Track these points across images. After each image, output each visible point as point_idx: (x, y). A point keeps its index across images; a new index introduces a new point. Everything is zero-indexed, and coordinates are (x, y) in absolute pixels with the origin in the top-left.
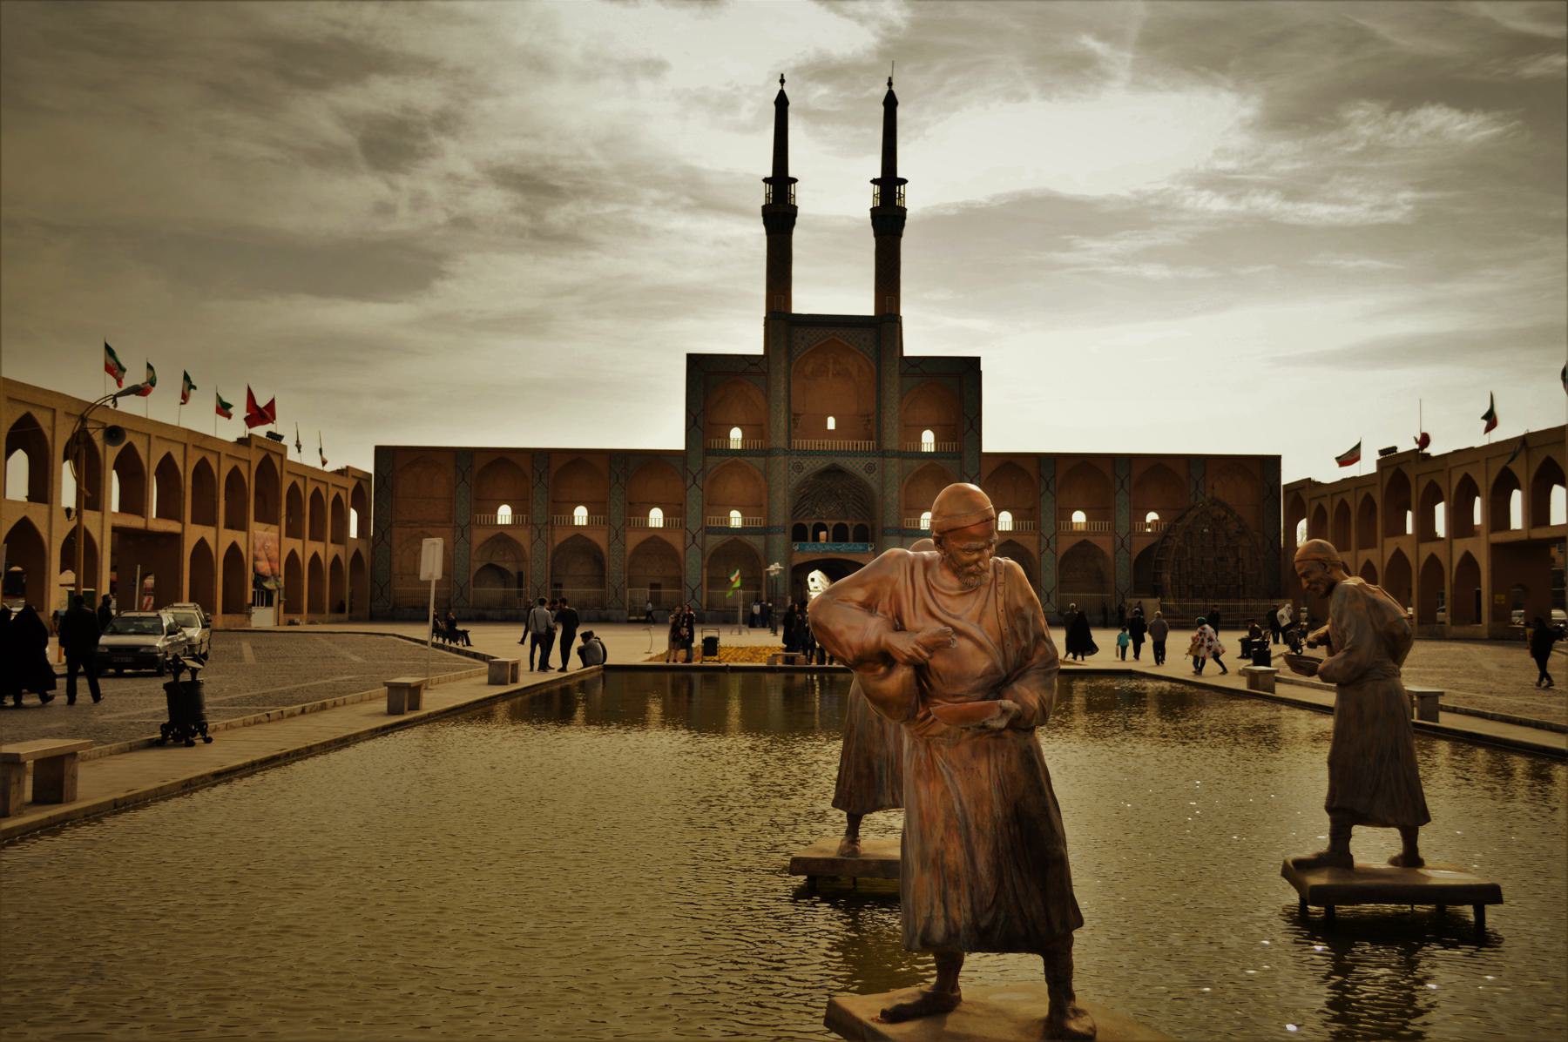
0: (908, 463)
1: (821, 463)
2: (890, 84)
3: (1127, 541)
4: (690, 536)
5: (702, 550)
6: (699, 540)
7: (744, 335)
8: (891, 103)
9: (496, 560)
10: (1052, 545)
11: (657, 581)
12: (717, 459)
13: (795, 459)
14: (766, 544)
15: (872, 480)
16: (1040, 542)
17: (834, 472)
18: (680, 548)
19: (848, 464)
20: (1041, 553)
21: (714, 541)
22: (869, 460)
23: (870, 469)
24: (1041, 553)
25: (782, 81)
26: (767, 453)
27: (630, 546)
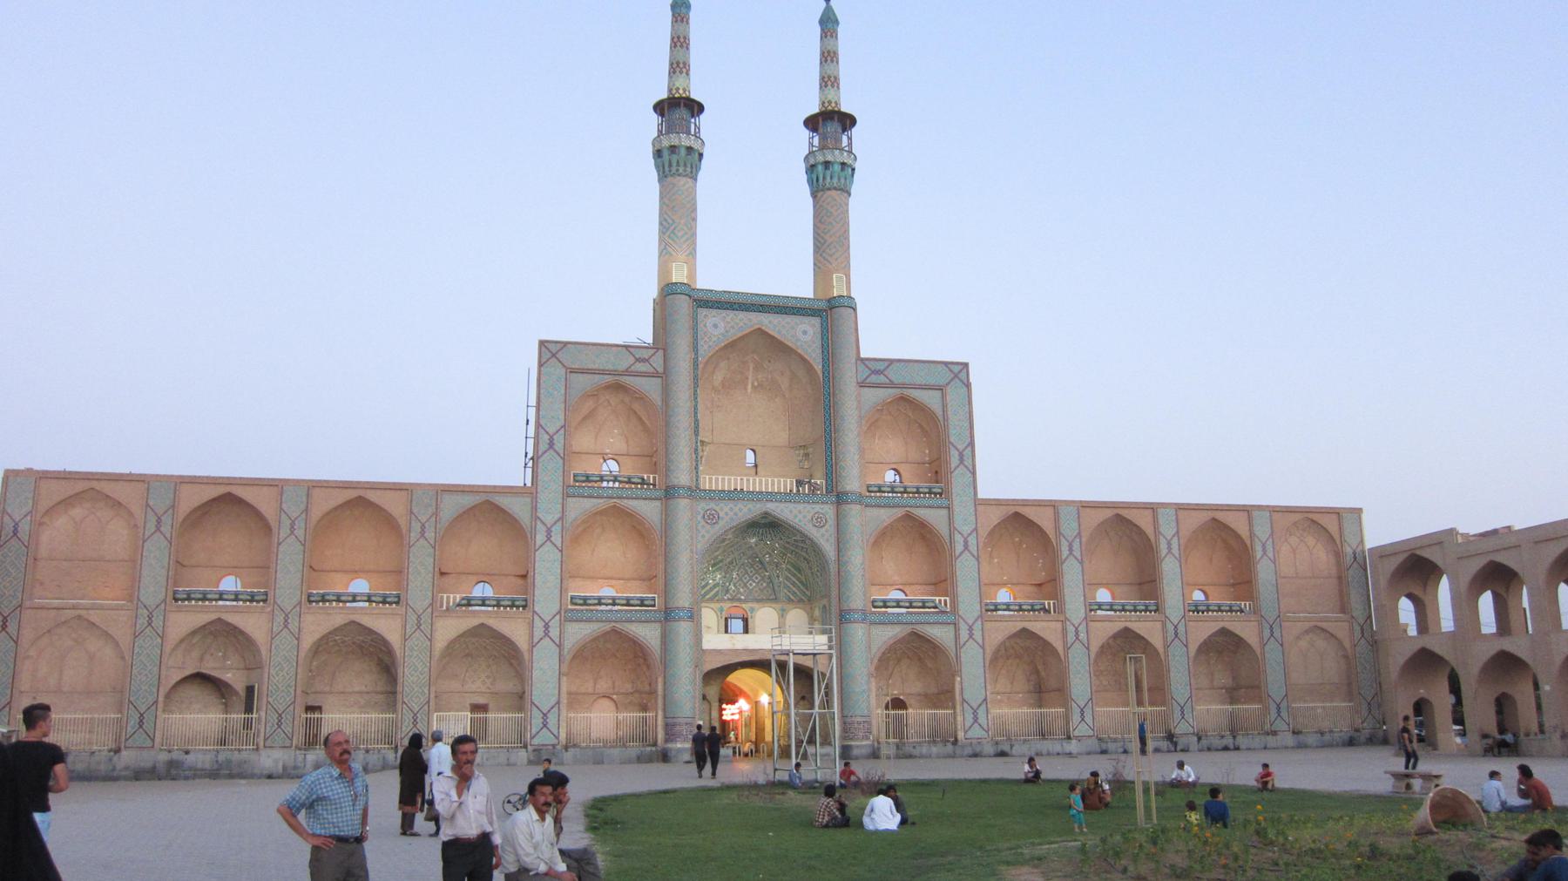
0: (875, 511)
3: (1181, 629)
4: (539, 624)
5: (560, 646)
6: (554, 633)
8: (828, 23)
9: (209, 668)
10: (1082, 636)
11: (481, 700)
13: (702, 506)
14: (665, 639)
18: (521, 641)
19: (784, 511)
20: (1067, 648)
21: (578, 633)
22: (818, 507)
23: (819, 522)
26: (669, 493)
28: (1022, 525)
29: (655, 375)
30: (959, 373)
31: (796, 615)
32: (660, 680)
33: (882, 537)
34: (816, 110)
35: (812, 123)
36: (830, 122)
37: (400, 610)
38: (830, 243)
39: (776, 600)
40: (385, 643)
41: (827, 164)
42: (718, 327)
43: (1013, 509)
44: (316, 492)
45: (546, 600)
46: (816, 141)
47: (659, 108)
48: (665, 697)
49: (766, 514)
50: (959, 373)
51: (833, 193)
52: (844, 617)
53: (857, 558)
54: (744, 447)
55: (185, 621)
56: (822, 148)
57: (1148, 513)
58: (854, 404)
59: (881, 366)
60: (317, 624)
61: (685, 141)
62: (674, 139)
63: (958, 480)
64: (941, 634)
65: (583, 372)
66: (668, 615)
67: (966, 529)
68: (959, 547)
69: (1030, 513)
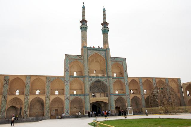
0: (113, 79)
1: (95, 79)
2: (104, 7)
4: (66, 97)
6: (68, 98)
7: (77, 51)
8: (104, 11)
9: (14, 105)
10: (143, 97)
12: (72, 78)
15: (107, 83)
16: (141, 96)
17: (98, 81)
18: (63, 99)
21: (72, 98)
23: (106, 81)
24: (142, 99)
25: (84, 4)
27: (51, 100)
28: (134, 81)
29: (82, 59)
30: (124, 59)
31: (102, 95)
32: (84, 105)
33: (115, 83)
34: (103, 22)
35: (102, 24)
36: (105, 24)
37: (45, 95)
38: (106, 41)
39: (99, 92)
40: (42, 100)
41: (105, 30)
42: (91, 53)
43: (133, 79)
44: (32, 77)
45: (67, 92)
46: (103, 27)
47: (81, 22)
48: (85, 107)
49: (98, 79)
50: (124, 59)
51: (106, 34)
52: (110, 94)
53: (112, 86)
54: (94, 70)
55: (10, 98)
56: (104, 27)
57: (151, 79)
58: (110, 64)
59: (114, 58)
60: (31, 98)
61: (85, 26)
62: (83, 26)
63: (125, 75)
64: (124, 97)
65: (72, 59)
66: (84, 95)
67: (127, 81)
68: (126, 84)
69: (135, 79)
